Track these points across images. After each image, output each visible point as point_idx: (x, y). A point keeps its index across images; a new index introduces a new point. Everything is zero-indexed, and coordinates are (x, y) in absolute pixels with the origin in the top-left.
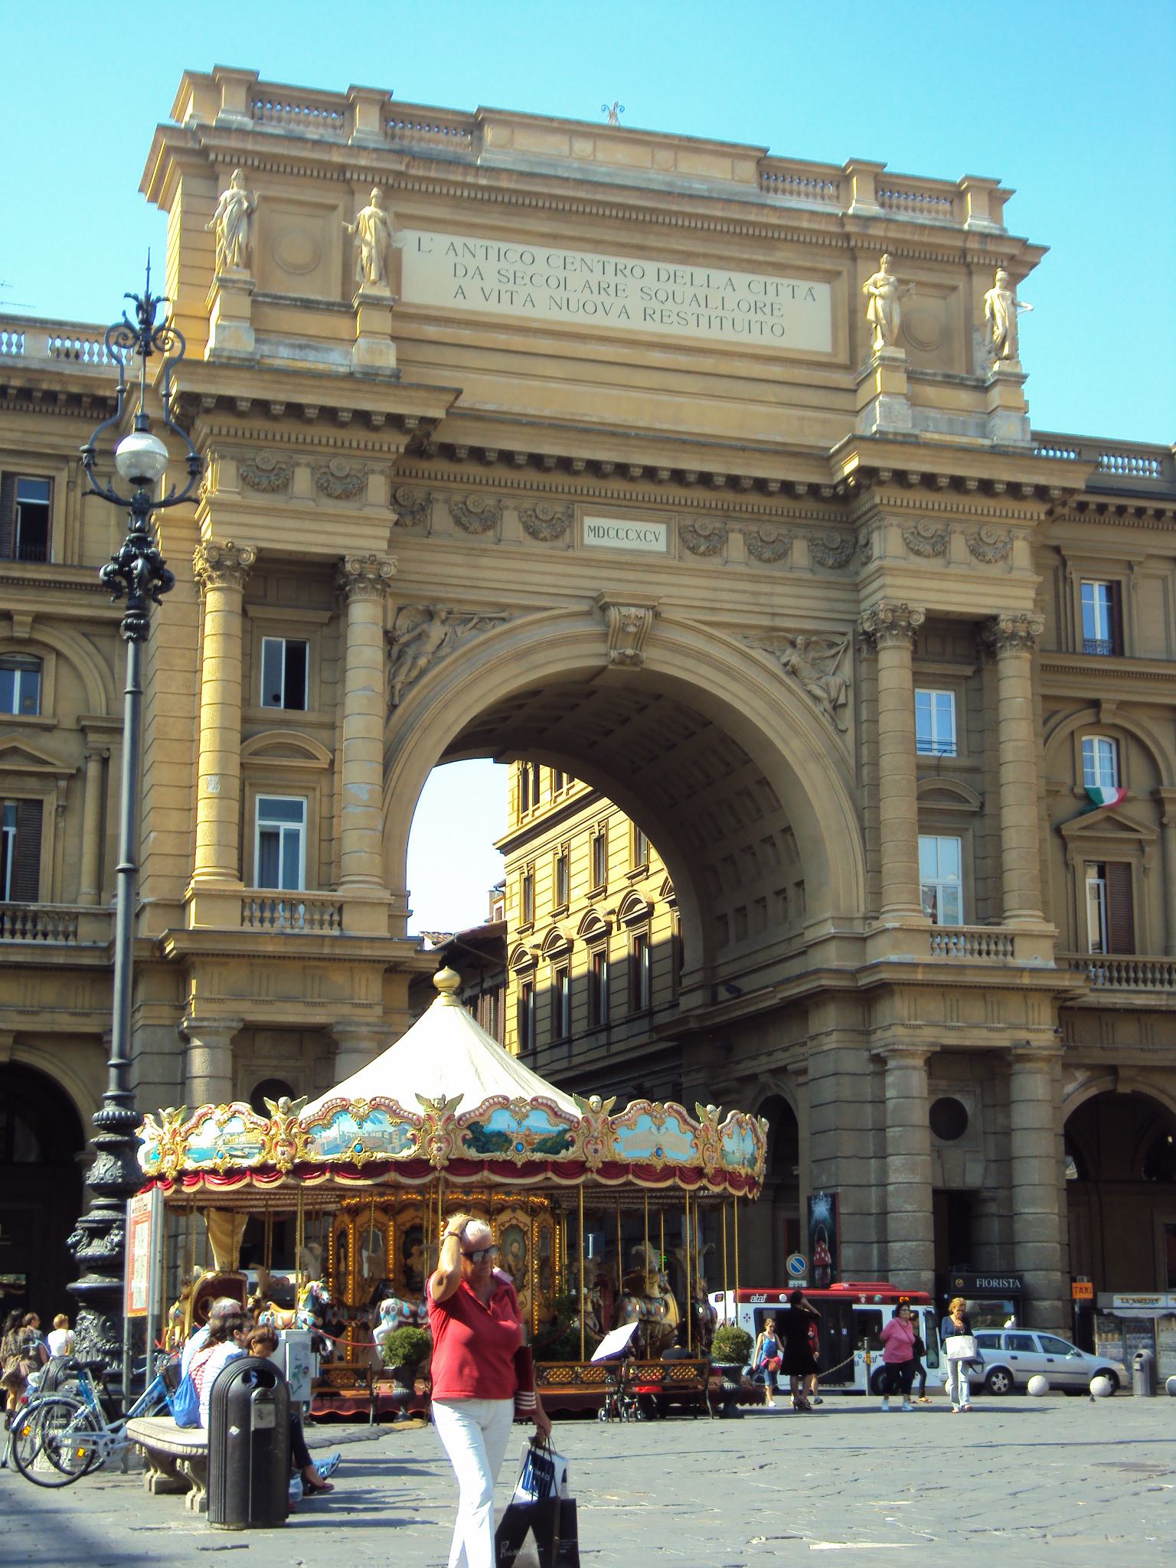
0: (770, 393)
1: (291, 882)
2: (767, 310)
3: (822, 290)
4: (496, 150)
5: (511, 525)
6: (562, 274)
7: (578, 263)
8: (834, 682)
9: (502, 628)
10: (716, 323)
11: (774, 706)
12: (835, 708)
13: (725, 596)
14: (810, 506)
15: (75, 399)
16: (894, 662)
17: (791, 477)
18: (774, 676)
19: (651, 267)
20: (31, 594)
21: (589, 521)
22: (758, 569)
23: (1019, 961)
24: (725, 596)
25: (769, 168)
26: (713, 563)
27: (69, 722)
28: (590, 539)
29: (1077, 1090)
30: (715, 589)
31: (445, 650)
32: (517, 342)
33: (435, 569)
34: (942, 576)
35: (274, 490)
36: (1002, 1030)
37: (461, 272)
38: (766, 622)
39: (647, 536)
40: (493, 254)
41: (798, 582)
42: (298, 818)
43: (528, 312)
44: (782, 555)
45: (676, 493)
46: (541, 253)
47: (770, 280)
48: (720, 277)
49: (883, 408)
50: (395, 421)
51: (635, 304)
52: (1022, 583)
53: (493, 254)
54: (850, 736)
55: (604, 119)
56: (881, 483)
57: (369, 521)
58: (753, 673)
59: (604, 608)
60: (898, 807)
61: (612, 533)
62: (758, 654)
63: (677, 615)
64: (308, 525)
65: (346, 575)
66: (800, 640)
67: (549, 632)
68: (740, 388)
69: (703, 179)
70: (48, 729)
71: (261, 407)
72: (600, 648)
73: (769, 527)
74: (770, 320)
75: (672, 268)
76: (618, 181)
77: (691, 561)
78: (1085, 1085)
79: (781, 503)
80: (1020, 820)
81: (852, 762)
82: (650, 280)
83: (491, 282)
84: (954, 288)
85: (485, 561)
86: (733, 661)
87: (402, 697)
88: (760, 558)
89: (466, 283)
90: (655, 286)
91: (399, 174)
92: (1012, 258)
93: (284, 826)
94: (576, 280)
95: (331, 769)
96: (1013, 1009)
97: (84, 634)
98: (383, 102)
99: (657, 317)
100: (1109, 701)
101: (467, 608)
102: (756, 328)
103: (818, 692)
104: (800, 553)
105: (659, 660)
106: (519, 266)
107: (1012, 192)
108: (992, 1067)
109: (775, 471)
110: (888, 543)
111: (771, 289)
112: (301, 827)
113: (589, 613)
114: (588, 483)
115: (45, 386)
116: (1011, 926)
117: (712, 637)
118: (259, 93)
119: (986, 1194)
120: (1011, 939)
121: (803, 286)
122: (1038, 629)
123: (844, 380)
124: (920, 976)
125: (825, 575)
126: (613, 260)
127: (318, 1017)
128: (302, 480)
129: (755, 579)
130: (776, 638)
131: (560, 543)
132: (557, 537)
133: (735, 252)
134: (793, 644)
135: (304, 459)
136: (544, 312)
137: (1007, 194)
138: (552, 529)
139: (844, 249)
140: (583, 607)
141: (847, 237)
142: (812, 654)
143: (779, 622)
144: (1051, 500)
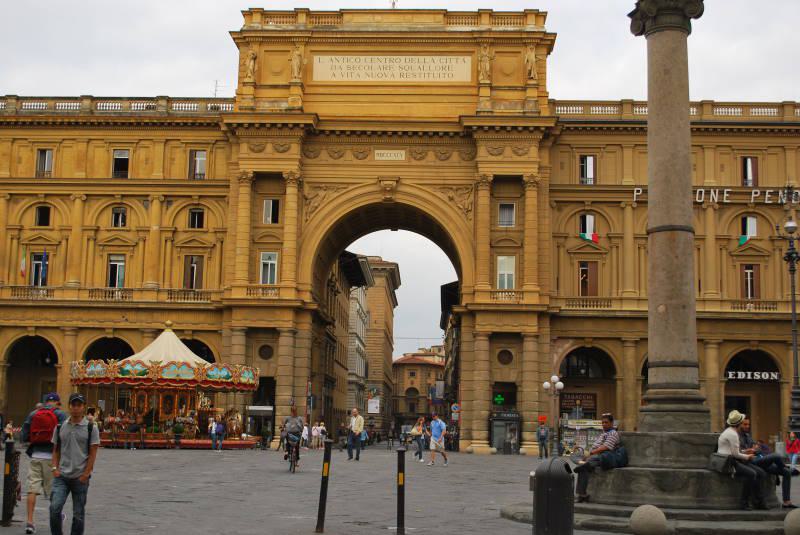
0: (445, 99)
1: (272, 282)
3: (468, 59)
4: (350, 24)
8: (467, 202)
9: (345, 191)
11: (444, 212)
14: (458, 140)
15: (209, 124)
16: (484, 196)
21: (377, 152)
22: (439, 163)
26: (423, 162)
27: (211, 230)
28: (377, 158)
29: (567, 347)
38: (441, 182)
39: (398, 155)
43: (358, 79)
44: (448, 158)
45: (407, 140)
46: (362, 58)
48: (428, 59)
51: (397, 72)
54: (472, 222)
55: (389, 6)
58: (436, 201)
60: (484, 248)
62: (439, 194)
69: (422, 23)
70: (207, 232)
72: (379, 196)
76: (390, 29)
77: (414, 162)
78: (573, 345)
79: (446, 140)
80: (530, 248)
82: (403, 63)
84: (519, 52)
92: (541, 39)
93: (270, 262)
94: (375, 66)
95: (282, 243)
96: (523, 319)
98: (308, 12)
104: (455, 157)
105: (400, 199)
107: (546, 13)
108: (518, 337)
109: (441, 129)
110: (482, 152)
114: (375, 139)
116: (525, 288)
118: (265, 14)
119: (517, 384)
120: (523, 292)
121: (461, 58)
122: (537, 179)
123: (474, 91)
124: (482, 308)
125: (464, 163)
127: (272, 325)
128: (269, 148)
129: (435, 167)
130: (445, 187)
133: (434, 49)
136: (364, 79)
139: (475, 41)
142: (460, 192)
143: (447, 182)
144: (542, 132)
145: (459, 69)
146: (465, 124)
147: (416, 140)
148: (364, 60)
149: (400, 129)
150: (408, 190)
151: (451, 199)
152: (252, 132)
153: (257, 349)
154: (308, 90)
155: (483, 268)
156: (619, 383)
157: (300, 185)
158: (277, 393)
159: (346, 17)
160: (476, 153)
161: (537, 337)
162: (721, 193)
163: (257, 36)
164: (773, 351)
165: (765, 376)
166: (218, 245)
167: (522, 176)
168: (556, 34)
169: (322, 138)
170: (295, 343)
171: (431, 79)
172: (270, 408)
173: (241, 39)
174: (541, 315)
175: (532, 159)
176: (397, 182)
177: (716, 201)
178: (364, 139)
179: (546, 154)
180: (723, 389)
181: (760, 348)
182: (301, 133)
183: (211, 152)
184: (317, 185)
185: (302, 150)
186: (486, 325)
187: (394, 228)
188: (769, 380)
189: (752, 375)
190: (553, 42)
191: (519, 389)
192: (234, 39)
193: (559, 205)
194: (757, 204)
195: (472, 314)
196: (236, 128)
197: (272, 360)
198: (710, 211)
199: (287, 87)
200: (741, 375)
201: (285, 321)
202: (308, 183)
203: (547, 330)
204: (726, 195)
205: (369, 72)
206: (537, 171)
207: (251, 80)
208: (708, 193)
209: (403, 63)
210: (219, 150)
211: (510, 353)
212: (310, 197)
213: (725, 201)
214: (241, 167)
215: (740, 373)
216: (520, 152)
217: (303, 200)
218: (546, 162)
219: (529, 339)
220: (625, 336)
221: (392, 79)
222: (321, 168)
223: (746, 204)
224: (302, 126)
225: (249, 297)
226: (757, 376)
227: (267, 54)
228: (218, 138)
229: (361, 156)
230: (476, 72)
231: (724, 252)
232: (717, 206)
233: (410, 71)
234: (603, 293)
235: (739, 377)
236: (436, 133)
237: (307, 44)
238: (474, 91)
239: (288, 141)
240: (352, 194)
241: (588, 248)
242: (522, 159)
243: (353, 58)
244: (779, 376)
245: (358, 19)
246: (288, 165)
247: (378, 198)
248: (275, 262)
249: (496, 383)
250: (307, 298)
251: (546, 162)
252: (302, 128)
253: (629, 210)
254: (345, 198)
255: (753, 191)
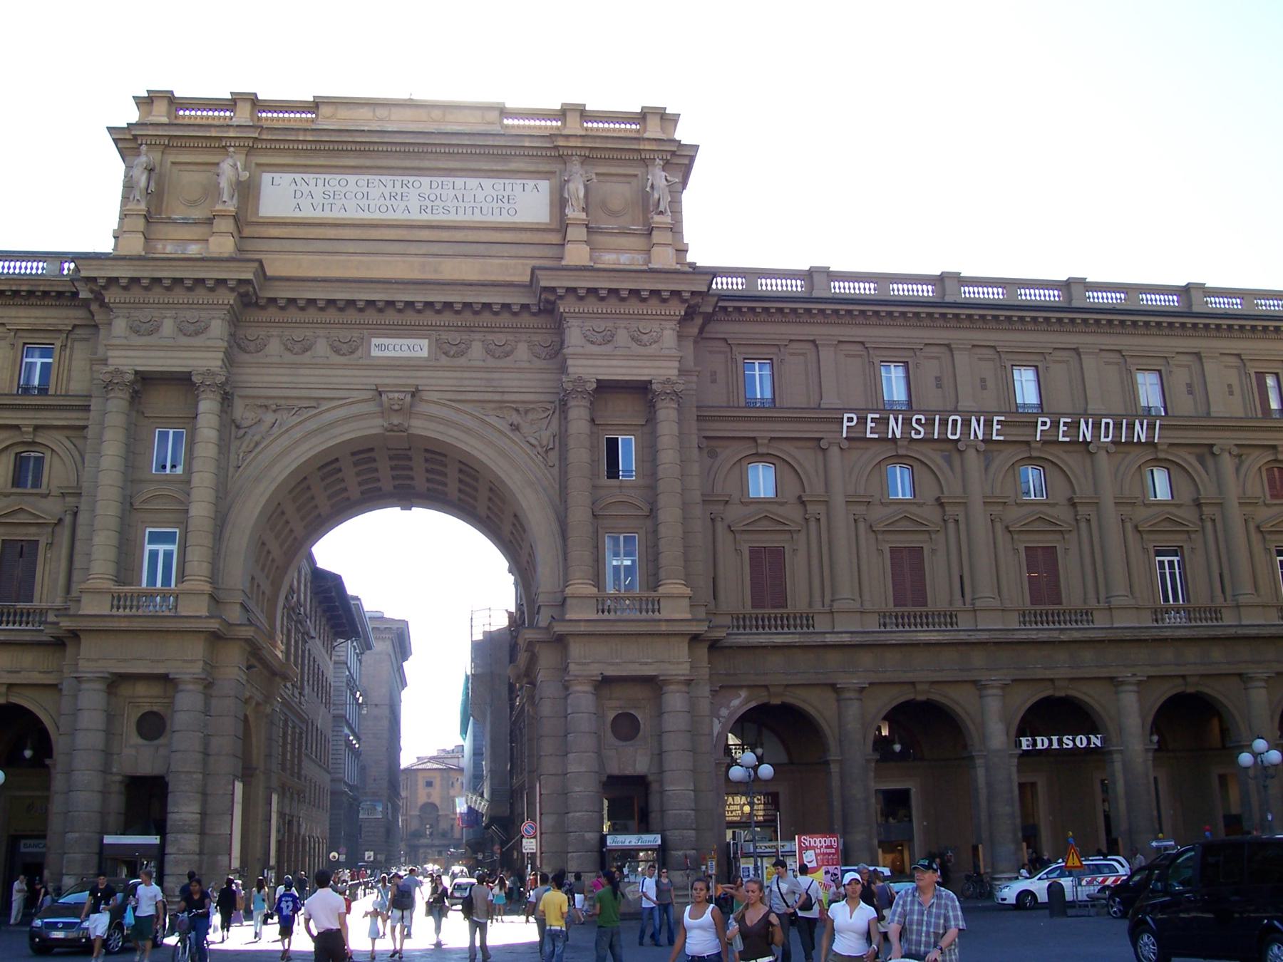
2: (505, 200)
3: (544, 185)
5: (322, 348)
6: (365, 190)
7: (376, 183)
10: (469, 211)
12: (547, 452)
13: (467, 383)
14: (526, 319)
16: (579, 414)
17: (508, 301)
18: (501, 432)
19: (426, 180)
20: (31, 414)
21: (375, 341)
22: (491, 362)
23: (665, 614)
24: (467, 383)
25: (503, 112)
26: (462, 361)
27: (55, 492)
28: (375, 352)
29: (739, 703)
30: (462, 379)
31: (275, 429)
32: (332, 233)
33: (266, 378)
34: (609, 357)
35: (151, 333)
36: (651, 664)
37: (298, 194)
38: (497, 397)
39: (418, 348)
40: (320, 183)
41: (520, 370)
42: (173, 542)
43: (342, 215)
45: (430, 318)
46: (352, 179)
47: (507, 181)
48: (472, 183)
49: (577, 254)
50: (221, 282)
51: (414, 203)
52: (669, 358)
53: (320, 183)
54: (555, 471)
56: (561, 297)
57: (208, 349)
59: (380, 394)
61: (391, 347)
63: (434, 396)
64: (170, 354)
65: (193, 384)
66: (521, 407)
67: (342, 413)
68: (482, 249)
71: (135, 281)
72: (379, 421)
73: (501, 335)
74: (507, 206)
75: (439, 180)
77: (444, 360)
78: (747, 701)
79: (505, 319)
80: (669, 514)
81: (557, 487)
82: (426, 190)
83: (318, 199)
84: (636, 176)
85: (302, 371)
86: (471, 423)
87: (244, 460)
88: (493, 356)
89: (302, 202)
90: (428, 191)
91: (256, 138)
92: (673, 153)
93: (161, 548)
97: (68, 438)
99: (429, 210)
100: (763, 438)
101: (290, 402)
102: (497, 211)
103: (533, 441)
104: (522, 351)
105: (419, 427)
106: (338, 188)
109: (495, 298)
110: (574, 336)
111: (508, 188)
112: (174, 548)
113: (372, 399)
114: (371, 316)
115: (41, 288)
117: (458, 409)
122: (678, 388)
123: (555, 238)
125: (539, 363)
126: (400, 178)
128: (168, 327)
131: (355, 356)
132: (352, 353)
134: (517, 410)
135: (169, 313)
137: (674, 119)
138: (348, 349)
140: (369, 395)
141: (556, 147)
142: (530, 416)
143: (507, 397)
145: (528, 202)
146: (543, 283)
147: (447, 318)
148: (353, 182)
149: (419, 297)
150: (434, 410)
151: (515, 428)
152: (136, 294)
153: (134, 719)
154: (247, 231)
155: (580, 554)
156: (834, 768)
157: (227, 399)
158: (170, 808)
159: (324, 110)
160: (563, 342)
161: (688, 683)
162: (989, 424)
163: (164, 140)
164: (1092, 696)
165: (1081, 741)
166: (68, 519)
167: (650, 382)
168: (697, 147)
169: (272, 313)
170: (207, 704)
171: (478, 217)
172: (155, 840)
173: (127, 141)
174: (695, 638)
175: (666, 352)
176: (413, 394)
177: (980, 437)
178: (351, 315)
179: (689, 346)
180: (1014, 769)
181: (1072, 693)
182: (231, 298)
183: (64, 347)
184: (259, 402)
185: (232, 335)
186: (589, 660)
187: (407, 506)
188: (1087, 749)
189: (1060, 742)
190: (692, 159)
191: (655, 787)
192: (116, 141)
193: (710, 445)
194: (1044, 442)
195: (561, 641)
196: (104, 288)
197: (162, 741)
198: (972, 459)
199: (209, 221)
200: (1042, 743)
201: (186, 660)
202: (240, 397)
203: (705, 671)
204: (996, 427)
205: (363, 203)
206: (676, 372)
207: (147, 205)
208: (966, 423)
209: (426, 190)
210: (77, 345)
211: (633, 719)
212: (245, 424)
213: (995, 438)
214: (110, 361)
215: (1039, 739)
216: (645, 338)
217: (229, 427)
218: (690, 363)
219: (672, 687)
220: (841, 680)
221: (406, 216)
222: (271, 371)
223: (1028, 443)
224: (231, 284)
225: (114, 612)
226: (1068, 742)
227: (175, 169)
228: (77, 322)
229: (345, 348)
230: (560, 203)
231: (999, 526)
232: (982, 447)
233: (438, 202)
234: (798, 601)
235: (1039, 746)
236: (487, 306)
237: (250, 151)
238: (555, 238)
239: (204, 315)
240: (328, 417)
241: (765, 522)
242: (652, 350)
243: (334, 179)
244: (1103, 740)
245: (343, 113)
246: (204, 359)
247: (373, 426)
248: (174, 548)
249: (610, 777)
250: (234, 614)
251: (690, 363)
252: (232, 290)
253: (835, 451)
254: (312, 425)
255: (1040, 420)
